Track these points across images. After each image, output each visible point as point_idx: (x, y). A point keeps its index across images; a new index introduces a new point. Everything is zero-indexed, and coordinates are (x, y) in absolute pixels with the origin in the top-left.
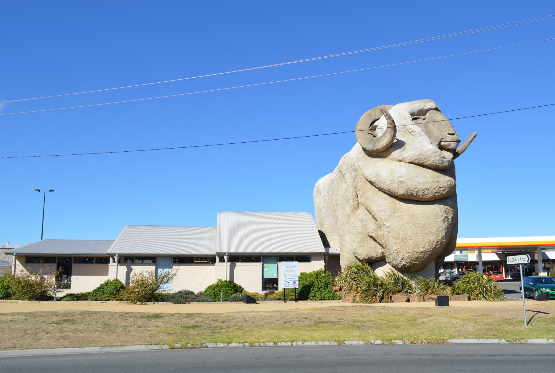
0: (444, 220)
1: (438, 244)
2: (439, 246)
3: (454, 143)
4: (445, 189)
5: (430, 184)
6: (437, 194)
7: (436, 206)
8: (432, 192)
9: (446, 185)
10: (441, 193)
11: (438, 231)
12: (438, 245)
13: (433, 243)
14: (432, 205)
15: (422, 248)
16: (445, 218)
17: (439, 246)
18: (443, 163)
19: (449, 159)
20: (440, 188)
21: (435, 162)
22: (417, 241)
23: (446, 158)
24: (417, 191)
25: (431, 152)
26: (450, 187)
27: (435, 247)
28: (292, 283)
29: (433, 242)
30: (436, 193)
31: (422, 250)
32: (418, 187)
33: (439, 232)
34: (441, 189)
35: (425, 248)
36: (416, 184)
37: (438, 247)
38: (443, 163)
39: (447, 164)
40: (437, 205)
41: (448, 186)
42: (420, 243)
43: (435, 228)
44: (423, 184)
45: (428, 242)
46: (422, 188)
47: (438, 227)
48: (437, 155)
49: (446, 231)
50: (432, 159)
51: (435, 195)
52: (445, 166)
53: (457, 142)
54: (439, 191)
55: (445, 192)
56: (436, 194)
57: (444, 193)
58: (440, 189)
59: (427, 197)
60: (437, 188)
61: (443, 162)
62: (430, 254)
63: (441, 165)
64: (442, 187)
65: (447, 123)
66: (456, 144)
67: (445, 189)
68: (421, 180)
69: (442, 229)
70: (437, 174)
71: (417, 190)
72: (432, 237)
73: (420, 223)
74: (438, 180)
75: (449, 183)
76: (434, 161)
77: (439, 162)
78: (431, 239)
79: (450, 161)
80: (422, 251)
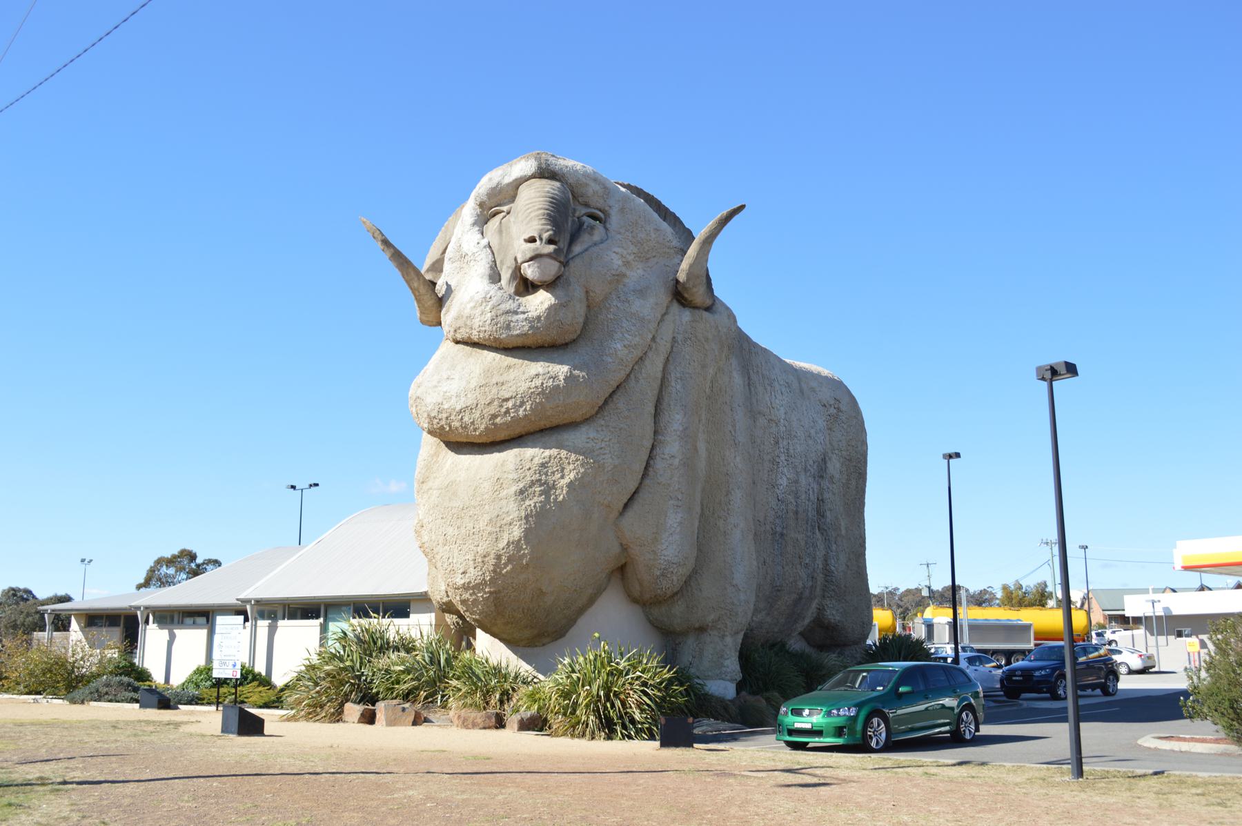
0: (521, 492)
1: (503, 562)
2: (508, 568)
3: (529, 266)
4: (522, 403)
5: (475, 396)
6: (499, 418)
7: (516, 451)
8: (482, 417)
9: (521, 390)
10: (512, 415)
11: (499, 525)
12: (506, 565)
13: (486, 559)
14: (505, 453)
15: (460, 576)
16: (530, 487)
17: (508, 568)
18: (508, 327)
19: (538, 311)
20: (507, 400)
21: (483, 329)
22: (447, 556)
23: (524, 313)
24: (447, 418)
25: (472, 304)
26: (543, 392)
27: (494, 571)
28: (231, 667)
29: (485, 556)
30: (494, 416)
31: (462, 582)
32: (446, 407)
33: (500, 527)
34: (510, 404)
35: (467, 575)
36: (440, 401)
37: (505, 570)
38: (508, 327)
39: (526, 328)
40: (515, 450)
41: (532, 390)
42: (454, 561)
43: (486, 517)
44: (457, 396)
45: (471, 557)
46: (452, 407)
47: (496, 514)
48: (488, 308)
49: (526, 523)
50: (477, 323)
51: (493, 424)
52: (518, 335)
53: (538, 260)
54: (503, 410)
55: (525, 410)
56: (498, 420)
57: (521, 412)
58: (505, 403)
59: (475, 430)
60: (496, 403)
61: (509, 325)
62: (490, 593)
63: (504, 336)
64: (511, 398)
65: (530, 210)
66: (536, 265)
67: (522, 403)
68: (454, 387)
69: (511, 517)
70: (510, 360)
71: (445, 415)
72: (480, 545)
73: (454, 506)
74: (504, 378)
75: (538, 382)
76: (481, 329)
77: (494, 329)
78: (479, 549)
79: (539, 318)
80: (464, 584)
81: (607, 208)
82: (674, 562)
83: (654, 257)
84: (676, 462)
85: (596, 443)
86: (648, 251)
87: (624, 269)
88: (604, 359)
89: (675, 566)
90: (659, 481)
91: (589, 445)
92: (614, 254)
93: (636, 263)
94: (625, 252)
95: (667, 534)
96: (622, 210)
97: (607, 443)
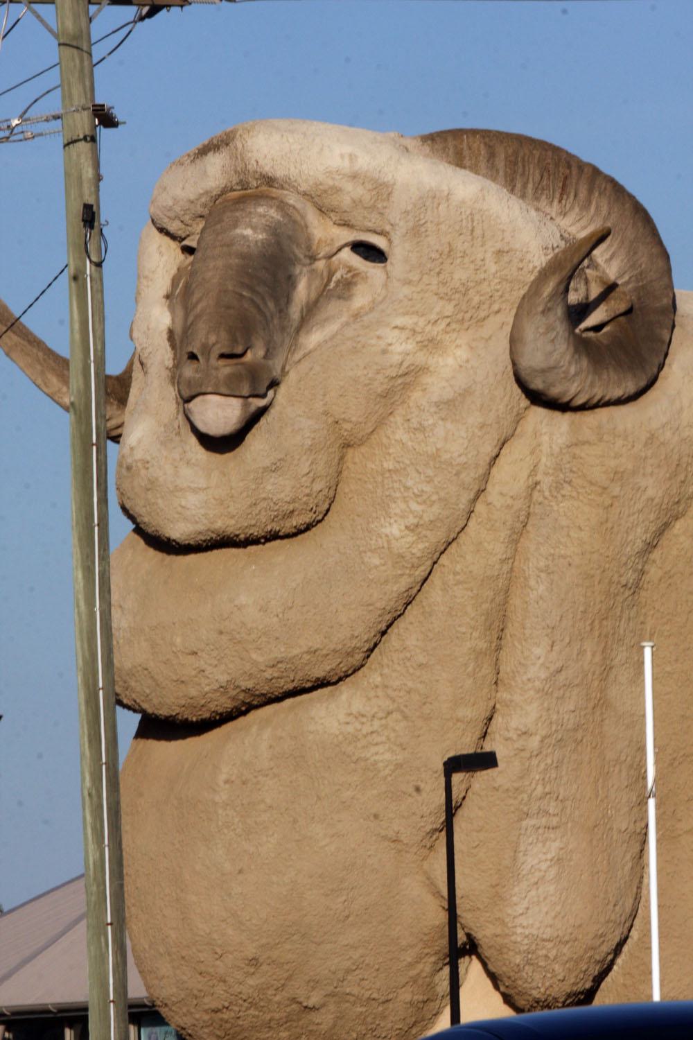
81: (388, 228)
82: (545, 936)
83: (498, 312)
84: (534, 742)
85: (363, 723)
86: (481, 303)
87: (420, 358)
88: (366, 559)
89: (550, 945)
90: (496, 785)
91: (350, 729)
92: (397, 332)
93: (454, 335)
94: (422, 322)
95: (524, 885)
96: (416, 231)
97: (384, 722)
